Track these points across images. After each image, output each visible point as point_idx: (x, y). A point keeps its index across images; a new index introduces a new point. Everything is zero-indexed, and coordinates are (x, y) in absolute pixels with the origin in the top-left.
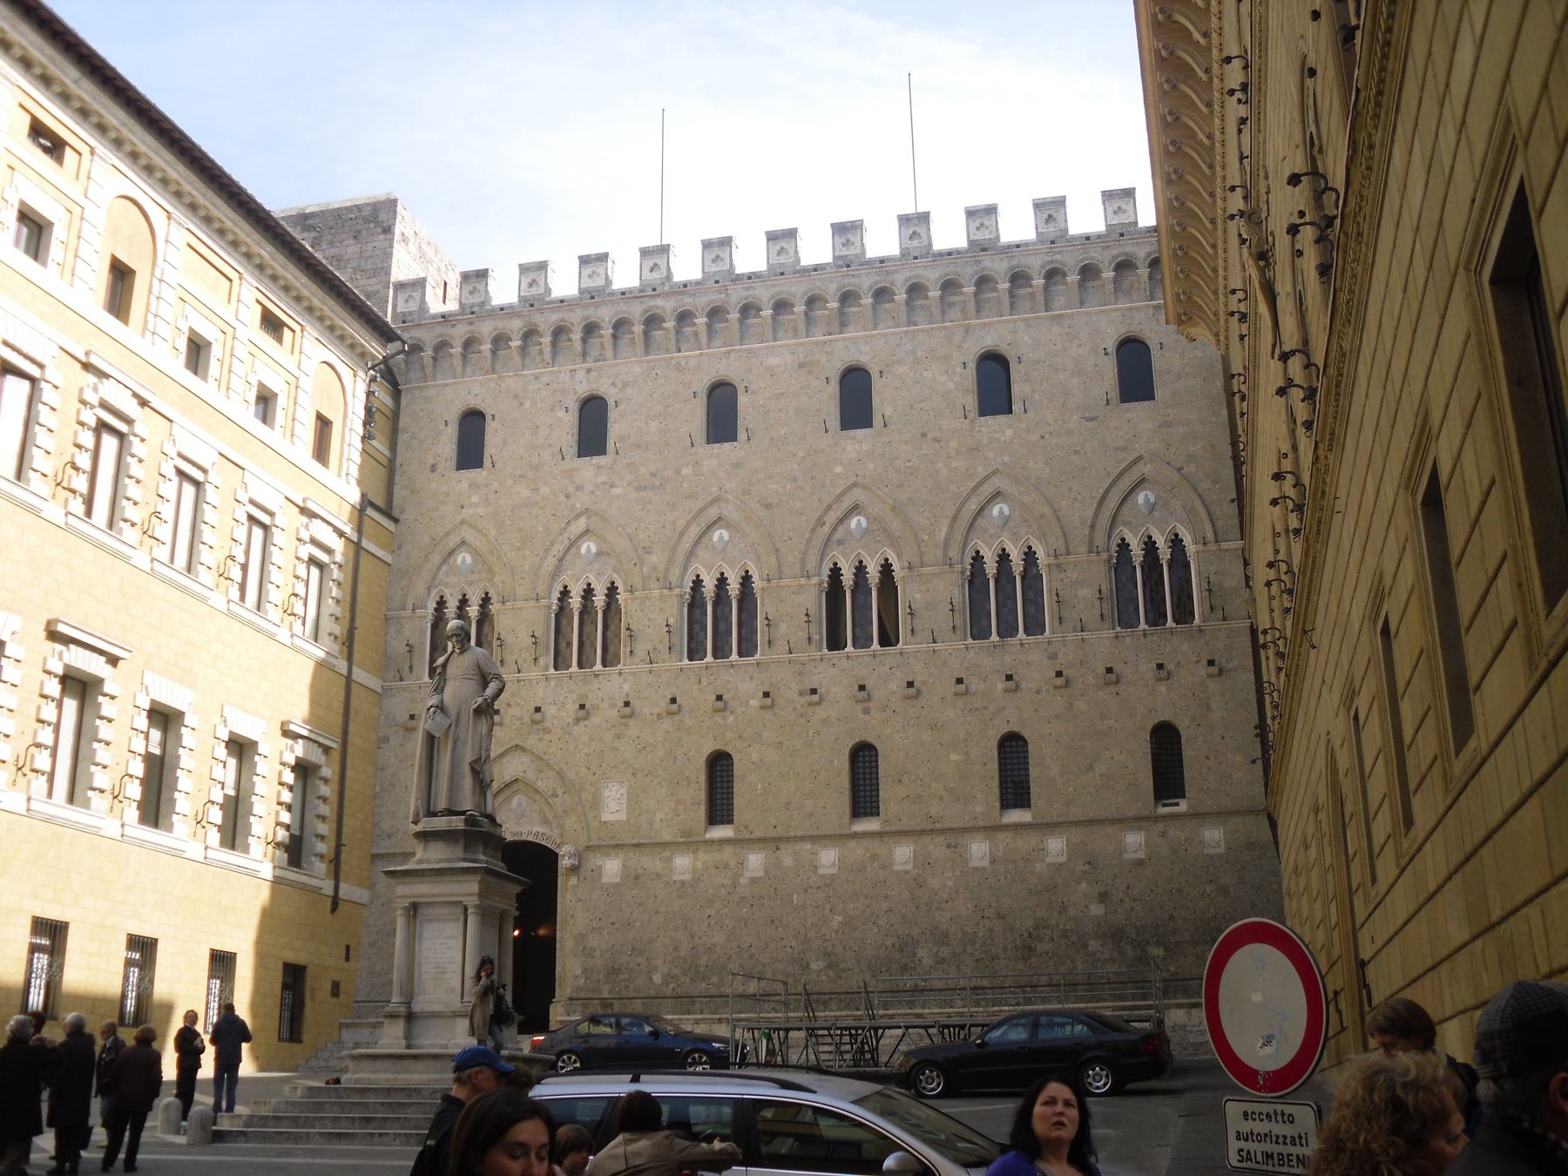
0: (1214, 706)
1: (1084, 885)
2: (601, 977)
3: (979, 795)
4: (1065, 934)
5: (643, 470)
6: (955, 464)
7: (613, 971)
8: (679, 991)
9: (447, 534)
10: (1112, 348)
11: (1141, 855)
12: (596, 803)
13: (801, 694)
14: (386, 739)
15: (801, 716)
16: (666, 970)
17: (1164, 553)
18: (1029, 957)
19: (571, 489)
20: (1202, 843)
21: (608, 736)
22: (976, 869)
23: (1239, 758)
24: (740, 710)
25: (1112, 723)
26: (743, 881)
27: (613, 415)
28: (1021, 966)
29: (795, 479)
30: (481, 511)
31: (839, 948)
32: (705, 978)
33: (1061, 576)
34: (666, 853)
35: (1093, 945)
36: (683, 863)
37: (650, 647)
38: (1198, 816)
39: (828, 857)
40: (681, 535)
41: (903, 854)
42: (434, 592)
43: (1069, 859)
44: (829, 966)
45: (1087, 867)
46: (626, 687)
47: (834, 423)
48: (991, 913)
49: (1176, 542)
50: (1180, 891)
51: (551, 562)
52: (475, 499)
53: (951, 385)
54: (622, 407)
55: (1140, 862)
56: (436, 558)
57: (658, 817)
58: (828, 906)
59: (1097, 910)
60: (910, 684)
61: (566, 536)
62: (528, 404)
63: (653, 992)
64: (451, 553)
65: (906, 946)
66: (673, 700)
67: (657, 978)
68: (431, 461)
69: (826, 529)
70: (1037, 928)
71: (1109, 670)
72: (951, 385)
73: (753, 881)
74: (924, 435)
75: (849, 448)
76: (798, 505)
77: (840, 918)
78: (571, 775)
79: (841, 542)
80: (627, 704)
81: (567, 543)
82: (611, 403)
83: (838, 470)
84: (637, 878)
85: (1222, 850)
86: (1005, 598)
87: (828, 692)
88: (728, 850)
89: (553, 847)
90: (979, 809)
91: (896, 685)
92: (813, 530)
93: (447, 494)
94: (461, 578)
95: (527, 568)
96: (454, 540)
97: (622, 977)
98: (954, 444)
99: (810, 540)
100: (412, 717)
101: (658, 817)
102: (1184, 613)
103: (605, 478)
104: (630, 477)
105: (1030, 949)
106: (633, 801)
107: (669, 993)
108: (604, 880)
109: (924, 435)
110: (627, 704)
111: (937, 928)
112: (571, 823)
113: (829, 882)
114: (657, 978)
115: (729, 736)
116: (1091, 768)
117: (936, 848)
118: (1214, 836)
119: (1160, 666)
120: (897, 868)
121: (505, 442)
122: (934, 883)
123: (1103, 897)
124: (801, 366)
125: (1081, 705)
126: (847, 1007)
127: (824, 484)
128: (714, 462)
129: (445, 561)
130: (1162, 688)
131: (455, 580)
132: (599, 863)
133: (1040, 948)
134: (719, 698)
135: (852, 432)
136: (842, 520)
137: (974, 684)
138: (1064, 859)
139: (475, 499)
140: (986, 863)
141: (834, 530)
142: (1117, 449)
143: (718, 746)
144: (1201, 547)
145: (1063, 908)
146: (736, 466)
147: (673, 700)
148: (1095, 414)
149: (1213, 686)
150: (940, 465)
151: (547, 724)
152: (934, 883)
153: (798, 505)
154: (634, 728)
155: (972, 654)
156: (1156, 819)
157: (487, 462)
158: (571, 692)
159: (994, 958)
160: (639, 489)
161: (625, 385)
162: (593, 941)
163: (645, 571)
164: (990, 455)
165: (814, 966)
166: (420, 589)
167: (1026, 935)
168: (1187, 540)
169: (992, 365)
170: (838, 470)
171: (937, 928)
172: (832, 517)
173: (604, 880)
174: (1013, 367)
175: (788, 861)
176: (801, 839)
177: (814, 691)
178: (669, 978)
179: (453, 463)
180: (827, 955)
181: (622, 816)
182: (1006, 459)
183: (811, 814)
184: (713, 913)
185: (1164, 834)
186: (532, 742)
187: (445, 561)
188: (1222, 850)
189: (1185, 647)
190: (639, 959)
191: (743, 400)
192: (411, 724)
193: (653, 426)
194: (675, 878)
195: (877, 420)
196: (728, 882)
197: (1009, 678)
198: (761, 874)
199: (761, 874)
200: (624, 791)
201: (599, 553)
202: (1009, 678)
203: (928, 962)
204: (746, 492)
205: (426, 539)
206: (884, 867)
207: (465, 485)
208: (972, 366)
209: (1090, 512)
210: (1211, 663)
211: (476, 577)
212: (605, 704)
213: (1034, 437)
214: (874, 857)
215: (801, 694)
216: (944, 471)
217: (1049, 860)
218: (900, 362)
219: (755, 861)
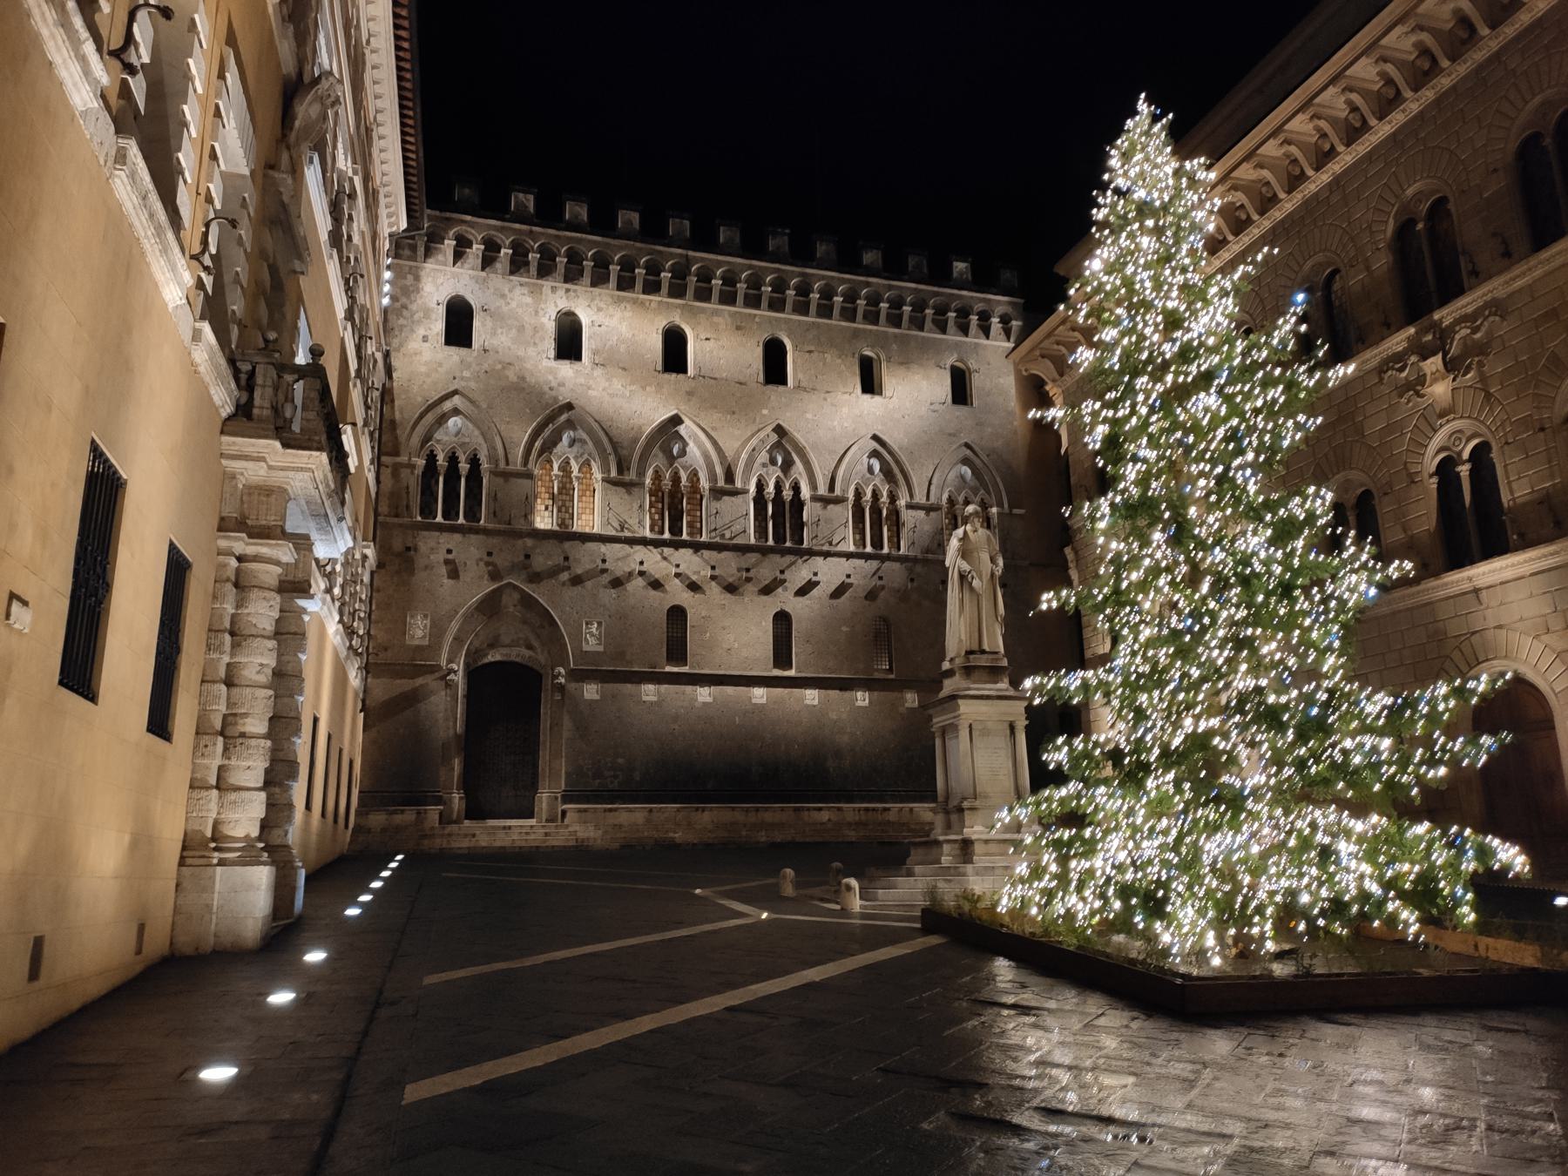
30: (473, 385)
100: (408, 549)
117: (834, 694)
194: (645, 698)
207: (456, 358)
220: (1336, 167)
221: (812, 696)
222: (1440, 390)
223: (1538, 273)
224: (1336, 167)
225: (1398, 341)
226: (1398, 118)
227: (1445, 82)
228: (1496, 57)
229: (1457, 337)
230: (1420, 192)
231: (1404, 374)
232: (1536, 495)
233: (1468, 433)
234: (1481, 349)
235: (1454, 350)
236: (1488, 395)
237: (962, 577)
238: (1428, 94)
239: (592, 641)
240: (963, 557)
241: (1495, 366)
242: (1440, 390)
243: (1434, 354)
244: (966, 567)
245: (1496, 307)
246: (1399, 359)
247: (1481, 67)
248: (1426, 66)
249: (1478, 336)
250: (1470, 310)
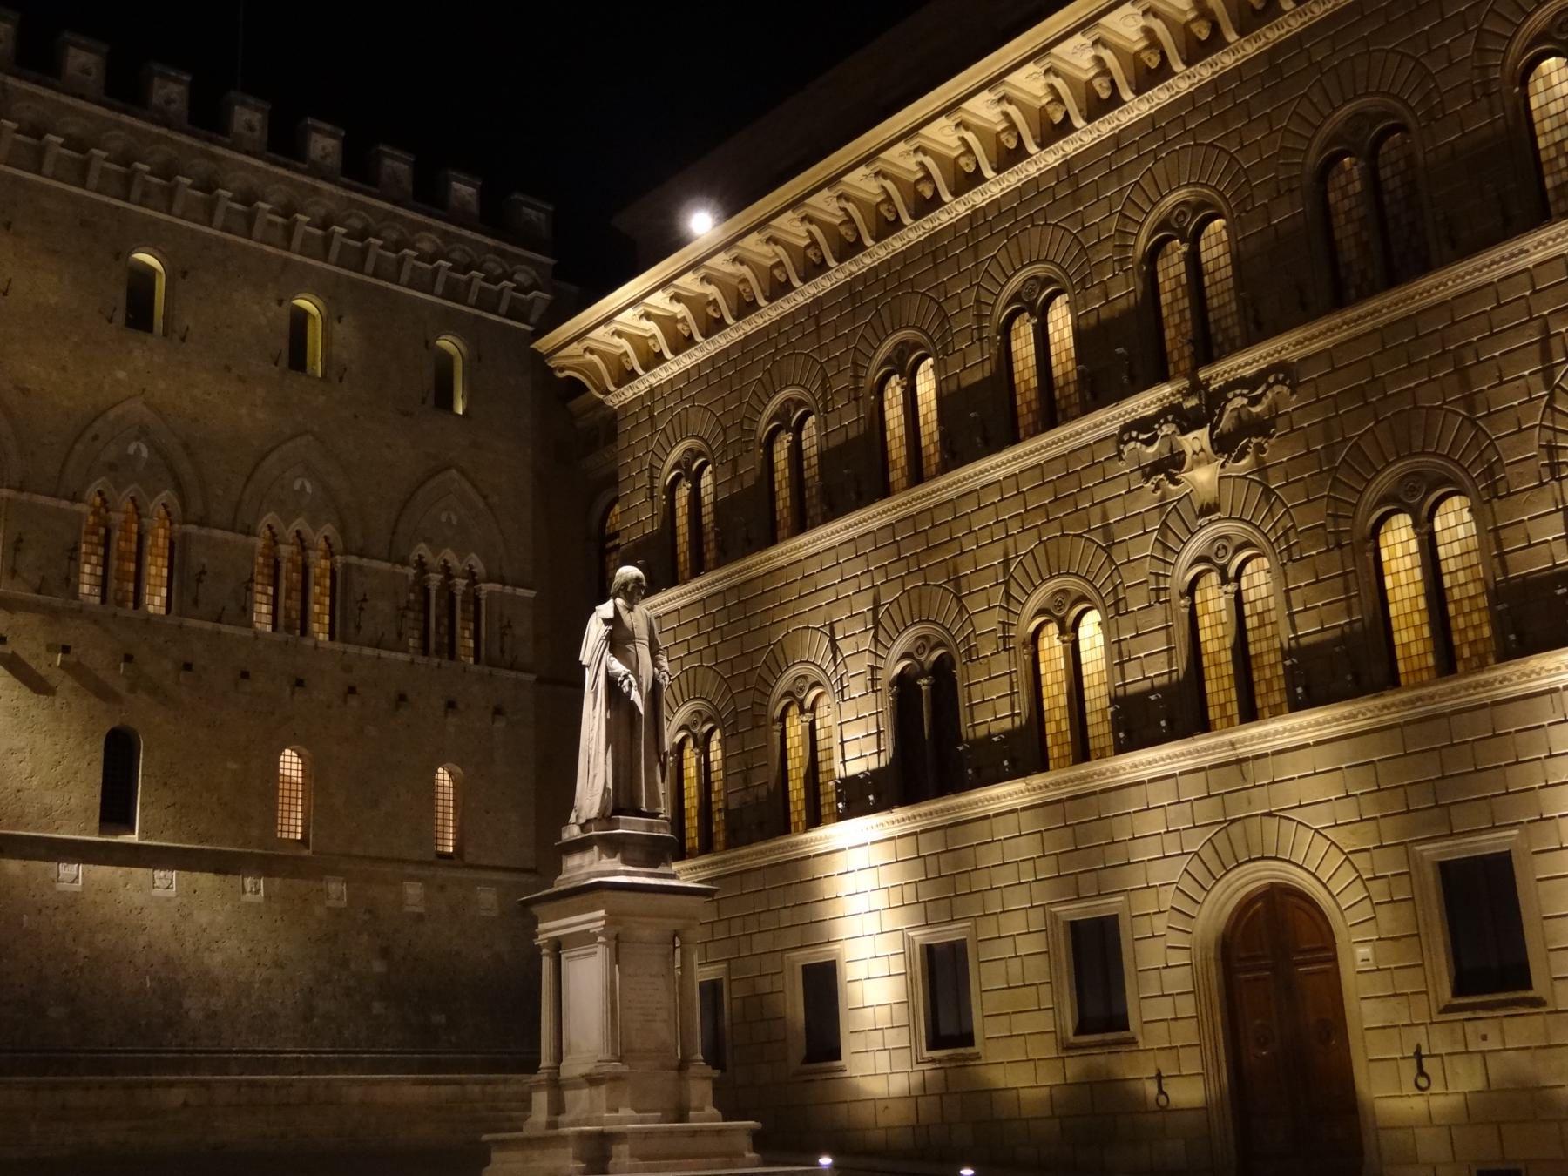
1: (365, 938)
29: (64, 369)
35: (377, 1007)
45: (366, 917)
53: (263, 320)
59: (378, 967)
72: (263, 320)
75: (137, 353)
83: (121, 375)
123: (385, 953)
138: (343, 903)
150: (243, 411)
152: (203, 918)
170: (121, 375)
188: (493, 914)
217: (329, 903)
220: (1068, 147)
221: (165, 882)
222: (1203, 477)
223: (1342, 336)
224: (1068, 147)
225: (1144, 403)
226: (1160, 96)
227: (1226, 61)
228: (1296, 40)
229: (1229, 407)
230: (1185, 203)
231: (1152, 450)
232: (1327, 635)
233: (1238, 541)
234: (1260, 427)
235: (1226, 423)
236: (1268, 492)
237: (612, 683)
238: (1205, 72)
240: (613, 651)
241: (1278, 452)
242: (1203, 477)
243: (1199, 426)
244: (618, 667)
245: (1282, 371)
246: (1144, 425)
247: (1277, 49)
248: (1204, 35)
249: (1257, 409)
250: (1248, 372)
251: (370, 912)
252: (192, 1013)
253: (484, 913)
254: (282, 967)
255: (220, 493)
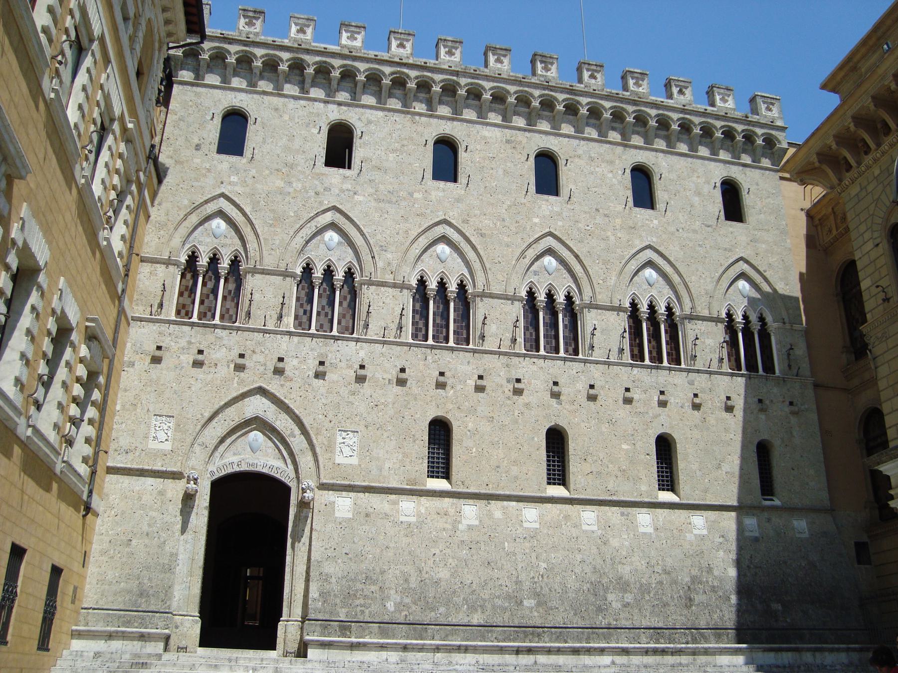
0: (795, 434)
1: (721, 553)
2: (338, 601)
3: (643, 477)
4: (714, 589)
5: (381, 187)
6: (619, 235)
7: (349, 596)
8: (411, 619)
9: (207, 202)
10: (719, 185)
11: (757, 534)
12: (330, 448)
13: (508, 381)
14: (132, 364)
15: (509, 398)
16: (398, 599)
17: (756, 326)
18: (691, 606)
19: (320, 189)
20: (793, 529)
21: (344, 391)
22: (645, 534)
23: (812, 472)
24: (459, 387)
25: (732, 436)
26: (460, 526)
27: (357, 142)
28: (685, 612)
29: (503, 220)
30: (239, 189)
31: (546, 590)
32: (433, 609)
33: (694, 327)
34: (393, 497)
36: (408, 506)
37: (384, 325)
38: (790, 510)
39: (531, 513)
40: (413, 242)
41: (589, 516)
42: (187, 246)
43: (709, 532)
44: (539, 604)
45: (721, 540)
46: (362, 354)
47: (533, 188)
48: (658, 569)
49: (762, 319)
50: (785, 562)
51: (299, 241)
52: (234, 179)
54: (365, 137)
55: (756, 540)
56: (194, 219)
57: (387, 466)
58: (534, 555)
60: (592, 387)
61: (313, 223)
62: (286, 117)
63: (386, 618)
64: (208, 218)
65: (598, 589)
66: (403, 370)
67: (390, 606)
68: (196, 141)
69: (527, 261)
70: (693, 582)
71: (728, 398)
73: (470, 528)
74: (597, 210)
76: (506, 239)
77: (544, 565)
78: (306, 422)
79: (536, 273)
80: (362, 367)
81: (314, 229)
82: (357, 133)
83: (536, 220)
84: (367, 515)
85: (806, 535)
86: (655, 336)
87: (530, 384)
88: (447, 501)
89: (286, 481)
90: (644, 488)
91: (582, 386)
92: (518, 260)
93: (209, 170)
94: (216, 239)
95: (277, 242)
96: (211, 208)
97: (358, 602)
98: (618, 221)
99: (515, 265)
100: (159, 348)
101: (387, 466)
102: (769, 368)
103: (349, 187)
104: (372, 191)
105: (690, 599)
106: (365, 450)
107: (402, 620)
108: (337, 514)
109: (597, 210)
110: (362, 367)
111: (621, 578)
112: (306, 461)
113: (533, 535)
114: (390, 606)
115: (450, 406)
116: (719, 467)
118: (801, 525)
119: (760, 401)
120: (585, 527)
121: (264, 142)
122: (615, 543)
124: (508, 142)
125: (711, 420)
126: (557, 640)
127: (525, 229)
128: (441, 194)
129: (201, 223)
130: (763, 416)
131: (208, 240)
132: (332, 499)
133: (698, 598)
134: (442, 374)
135: (546, 197)
136: (539, 257)
137: (635, 394)
138: (705, 532)
139: (234, 179)
140: (650, 530)
141: (532, 264)
142: (726, 249)
143: (440, 413)
144: (781, 324)
145: (710, 570)
146: (459, 200)
147: (403, 370)
148: (710, 223)
149: (794, 420)
150: (609, 233)
151: (288, 373)
153: (506, 239)
154: (366, 389)
155: (636, 370)
156: (763, 509)
157: (248, 152)
158: (312, 350)
159: (666, 605)
160: (378, 200)
161: (369, 122)
162: (329, 568)
163: (380, 264)
164: (644, 234)
165: (526, 603)
166: (177, 241)
167: (686, 588)
168: (769, 319)
169: (637, 173)
170: (536, 220)
171: (621, 578)
172: (531, 254)
173: (337, 514)
174: (656, 179)
175: (498, 514)
176: (509, 498)
177: (518, 381)
178: (400, 606)
179: (215, 147)
180: (537, 595)
181: (354, 461)
182: (654, 240)
183: (516, 478)
184: (437, 552)
185: (769, 520)
186: (274, 386)
187: (201, 223)
189: (775, 390)
190: (373, 588)
191: (462, 156)
192: (158, 353)
193: (392, 156)
194: (403, 519)
195: (564, 191)
196: (449, 527)
197: (662, 393)
198: (477, 523)
199: (477, 523)
200: (355, 440)
201: (339, 243)
202: (662, 393)
203: (616, 605)
204: (466, 221)
205: (186, 202)
206: (576, 526)
208: (628, 171)
209: (710, 287)
210: (791, 403)
211: (228, 241)
212: (343, 364)
213: (672, 229)
214: (567, 517)
215: (508, 381)
216: (612, 238)
217: (696, 532)
218: (579, 157)
219: (470, 511)
239: (347, 451)
251: (723, 537)
252: (614, 604)
253: (797, 536)
254: (669, 573)
255: (601, 282)
